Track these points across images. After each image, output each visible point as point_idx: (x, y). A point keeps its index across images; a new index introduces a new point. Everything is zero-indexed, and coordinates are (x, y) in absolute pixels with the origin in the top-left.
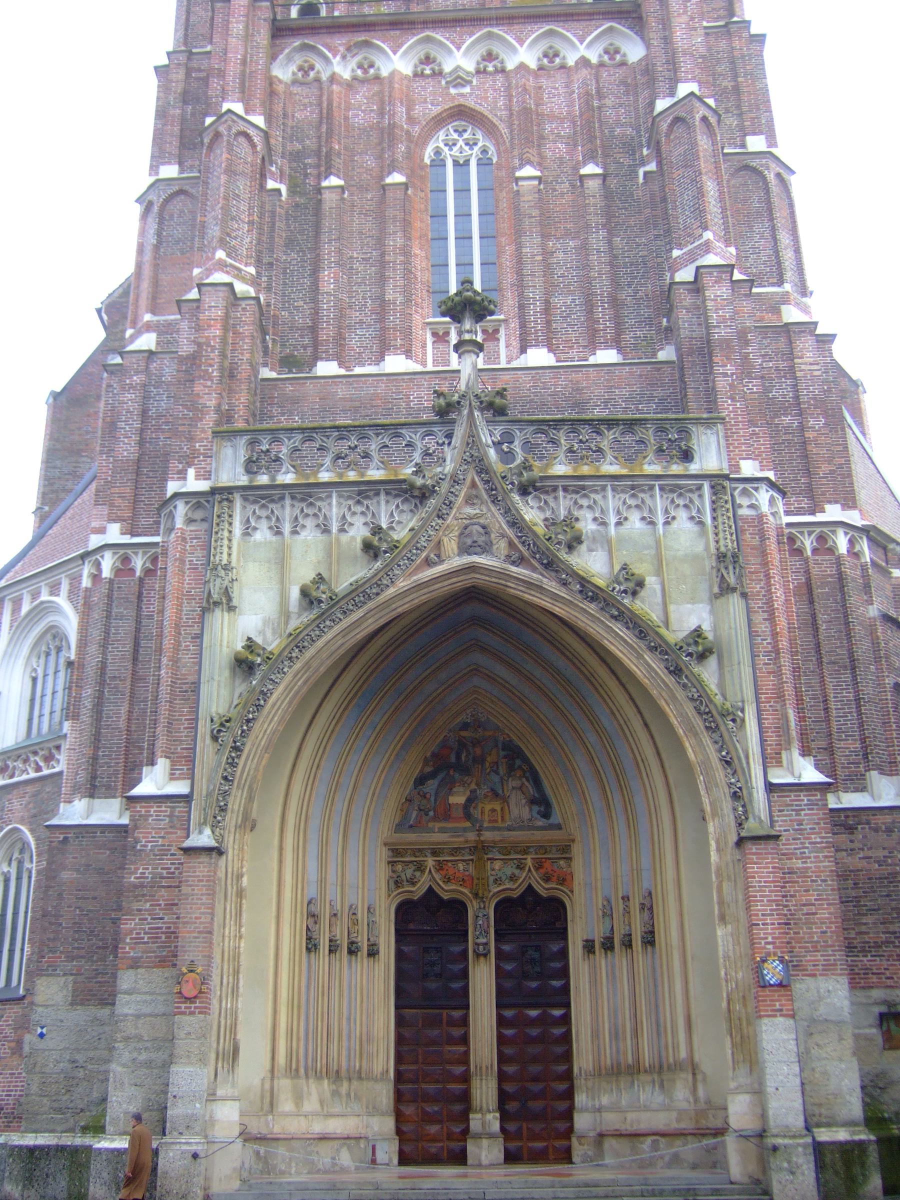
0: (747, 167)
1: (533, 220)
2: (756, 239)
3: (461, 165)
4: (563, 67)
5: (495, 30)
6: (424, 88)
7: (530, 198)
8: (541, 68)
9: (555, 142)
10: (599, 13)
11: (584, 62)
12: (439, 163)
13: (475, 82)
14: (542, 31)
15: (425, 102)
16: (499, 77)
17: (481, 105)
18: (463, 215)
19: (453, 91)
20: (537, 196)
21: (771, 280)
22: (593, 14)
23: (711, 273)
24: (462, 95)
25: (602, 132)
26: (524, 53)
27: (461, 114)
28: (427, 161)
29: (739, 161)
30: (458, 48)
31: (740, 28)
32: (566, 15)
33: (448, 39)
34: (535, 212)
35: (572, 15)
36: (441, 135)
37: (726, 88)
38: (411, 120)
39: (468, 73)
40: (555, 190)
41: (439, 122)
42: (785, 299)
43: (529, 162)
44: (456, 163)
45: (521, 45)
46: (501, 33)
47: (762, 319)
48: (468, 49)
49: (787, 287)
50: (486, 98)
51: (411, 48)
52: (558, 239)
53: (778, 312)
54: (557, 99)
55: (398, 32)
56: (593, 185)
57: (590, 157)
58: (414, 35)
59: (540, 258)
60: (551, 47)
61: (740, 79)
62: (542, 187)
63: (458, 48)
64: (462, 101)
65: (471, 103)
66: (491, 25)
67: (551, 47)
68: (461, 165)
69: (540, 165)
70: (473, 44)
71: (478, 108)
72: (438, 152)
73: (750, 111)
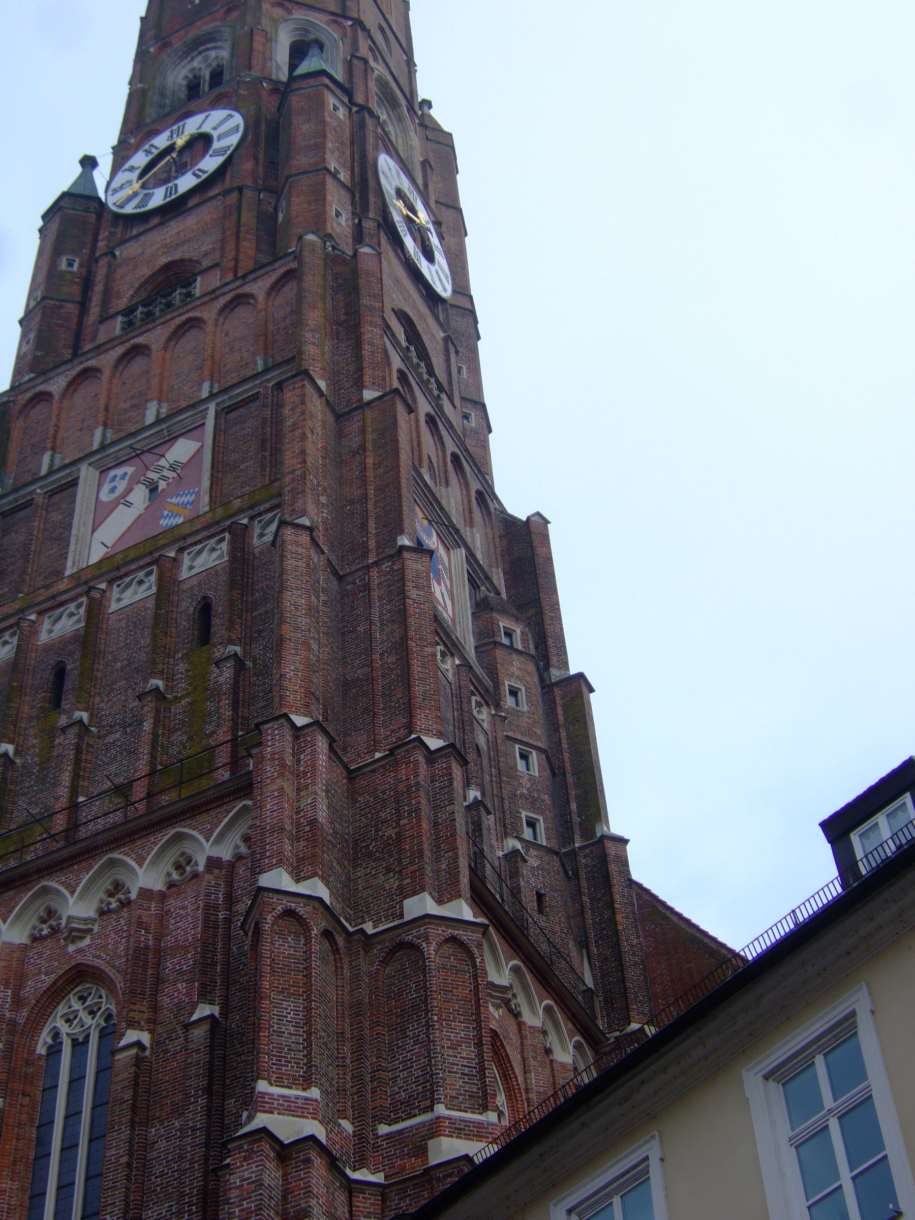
0: (402, 945)
1: (124, 1106)
2: (408, 1047)
3: (79, 1045)
4: (196, 875)
5: (115, 855)
6: (40, 954)
7: (125, 1075)
8: (171, 885)
9: (175, 982)
10: (228, 795)
11: (213, 863)
12: (54, 1050)
13: (96, 928)
14: (166, 838)
15: (40, 973)
16: (125, 913)
17: (99, 957)
18: (73, 1115)
19: (71, 948)
20: (133, 1069)
21: (423, 1104)
22: (222, 797)
23: (241, 1146)
24: (80, 951)
25: (227, 950)
26: (147, 875)
27: (79, 975)
28: (41, 1050)
29: (392, 939)
30: (72, 893)
31: (408, 751)
32: (192, 809)
33: (62, 883)
34: (128, 1095)
35: (198, 807)
36: (62, 1009)
37: (390, 837)
38: (18, 1001)
39: (85, 920)
40: (166, 1051)
41: (55, 994)
42: (435, 1129)
43: (133, 1024)
44: (75, 1043)
45: (141, 866)
46: (121, 856)
47: (403, 1168)
48: (86, 889)
49: (440, 1109)
50: (103, 949)
51: (25, 908)
52: (161, 1122)
53: (421, 1151)
54: (185, 925)
55: (11, 893)
56: (199, 1034)
57: (205, 996)
58: (29, 890)
59: (124, 1160)
60: (183, 854)
61: (402, 822)
62: (148, 1053)
63: (72, 893)
64: (80, 959)
65: (89, 959)
66: (111, 850)
67: (183, 854)
68: (79, 1045)
69: (152, 1025)
70: (92, 880)
71: (97, 962)
72: (56, 1035)
73: (412, 863)
